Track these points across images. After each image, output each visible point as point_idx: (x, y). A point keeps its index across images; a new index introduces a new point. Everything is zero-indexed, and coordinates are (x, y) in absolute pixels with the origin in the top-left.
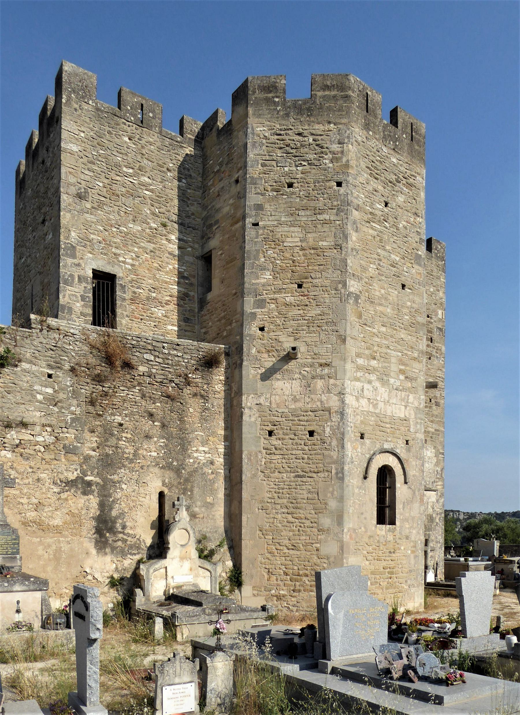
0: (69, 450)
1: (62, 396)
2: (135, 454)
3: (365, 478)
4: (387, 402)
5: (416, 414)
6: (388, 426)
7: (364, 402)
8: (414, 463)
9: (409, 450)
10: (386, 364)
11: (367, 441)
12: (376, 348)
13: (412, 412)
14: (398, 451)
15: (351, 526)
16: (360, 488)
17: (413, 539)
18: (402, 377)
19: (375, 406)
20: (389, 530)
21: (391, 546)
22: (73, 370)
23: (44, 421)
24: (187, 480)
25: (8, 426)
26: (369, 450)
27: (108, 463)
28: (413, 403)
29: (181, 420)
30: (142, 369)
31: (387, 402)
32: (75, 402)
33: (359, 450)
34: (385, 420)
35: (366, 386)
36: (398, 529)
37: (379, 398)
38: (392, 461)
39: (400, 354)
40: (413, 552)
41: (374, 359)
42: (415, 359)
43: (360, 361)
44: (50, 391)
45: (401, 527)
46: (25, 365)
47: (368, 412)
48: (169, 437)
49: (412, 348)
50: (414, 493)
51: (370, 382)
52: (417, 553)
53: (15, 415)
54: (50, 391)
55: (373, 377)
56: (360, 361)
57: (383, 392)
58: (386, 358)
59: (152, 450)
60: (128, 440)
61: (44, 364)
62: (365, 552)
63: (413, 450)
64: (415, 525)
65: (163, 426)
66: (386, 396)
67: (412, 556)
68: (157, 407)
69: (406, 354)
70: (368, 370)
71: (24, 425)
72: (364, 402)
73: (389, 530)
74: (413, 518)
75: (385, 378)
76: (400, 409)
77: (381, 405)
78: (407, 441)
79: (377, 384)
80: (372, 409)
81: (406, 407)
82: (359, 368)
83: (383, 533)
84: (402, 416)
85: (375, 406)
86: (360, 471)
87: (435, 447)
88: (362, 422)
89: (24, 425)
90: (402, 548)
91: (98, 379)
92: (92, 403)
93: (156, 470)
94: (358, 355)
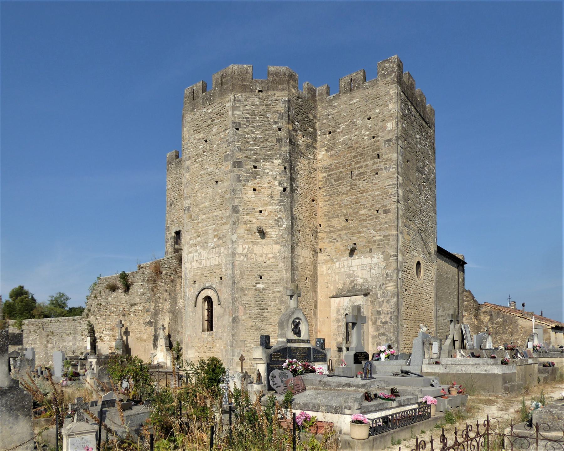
0: (148, 311)
1: (145, 291)
2: (163, 308)
3: (195, 306)
4: (207, 259)
5: (226, 258)
6: (208, 272)
7: (194, 264)
8: (225, 291)
9: (221, 283)
10: (206, 237)
11: (196, 285)
12: (199, 231)
13: (223, 258)
14: (214, 286)
15: (189, 333)
16: (192, 312)
17: (224, 339)
18: (215, 239)
19: (200, 264)
20: (209, 335)
21: (210, 344)
22: (148, 280)
23: (141, 302)
24: (176, 316)
25: (132, 306)
26: (198, 289)
27: (156, 313)
28: (223, 253)
29: (175, 290)
30: (164, 272)
31: (207, 259)
32: (148, 292)
33: (192, 291)
34: (206, 270)
35: (195, 254)
36: (214, 333)
37: (202, 258)
38: (209, 293)
39: (214, 226)
40: (224, 347)
41: (199, 236)
42: (224, 224)
43: (192, 242)
44: (142, 290)
45: (216, 332)
46: (135, 284)
47: (197, 268)
48: (171, 298)
49: (222, 218)
50: (225, 310)
51: (196, 251)
52: (227, 348)
53: (133, 302)
54: (142, 290)
55: (198, 248)
56: (192, 242)
57: (204, 253)
58: (206, 233)
59: (167, 306)
60: (162, 303)
61: (140, 281)
62: (196, 348)
63: (224, 282)
64: (226, 330)
65: (170, 294)
66: (206, 255)
67: (224, 350)
68: (168, 287)
69: (218, 224)
70: (196, 245)
71: (135, 304)
72: (194, 264)
73: (209, 335)
74: (224, 326)
75: (205, 245)
76: (215, 260)
77: (204, 261)
78: (221, 278)
79: (201, 251)
80: (199, 266)
81: (219, 257)
82: (191, 246)
83: (206, 336)
84: (217, 263)
85: (200, 264)
86: (193, 302)
87: (383, 253)
88: (194, 275)
89: (135, 304)
90: (218, 345)
91: (154, 281)
92: (153, 291)
93: (167, 314)
94: (191, 239)
